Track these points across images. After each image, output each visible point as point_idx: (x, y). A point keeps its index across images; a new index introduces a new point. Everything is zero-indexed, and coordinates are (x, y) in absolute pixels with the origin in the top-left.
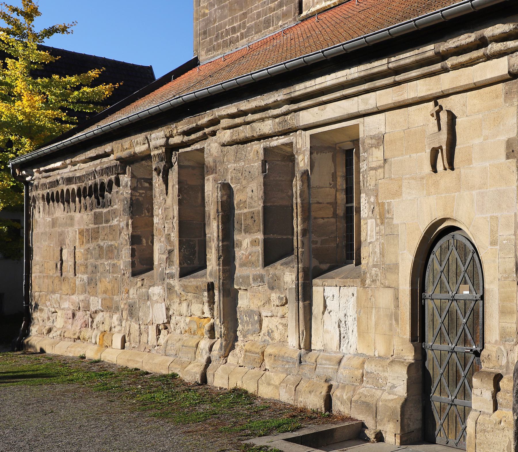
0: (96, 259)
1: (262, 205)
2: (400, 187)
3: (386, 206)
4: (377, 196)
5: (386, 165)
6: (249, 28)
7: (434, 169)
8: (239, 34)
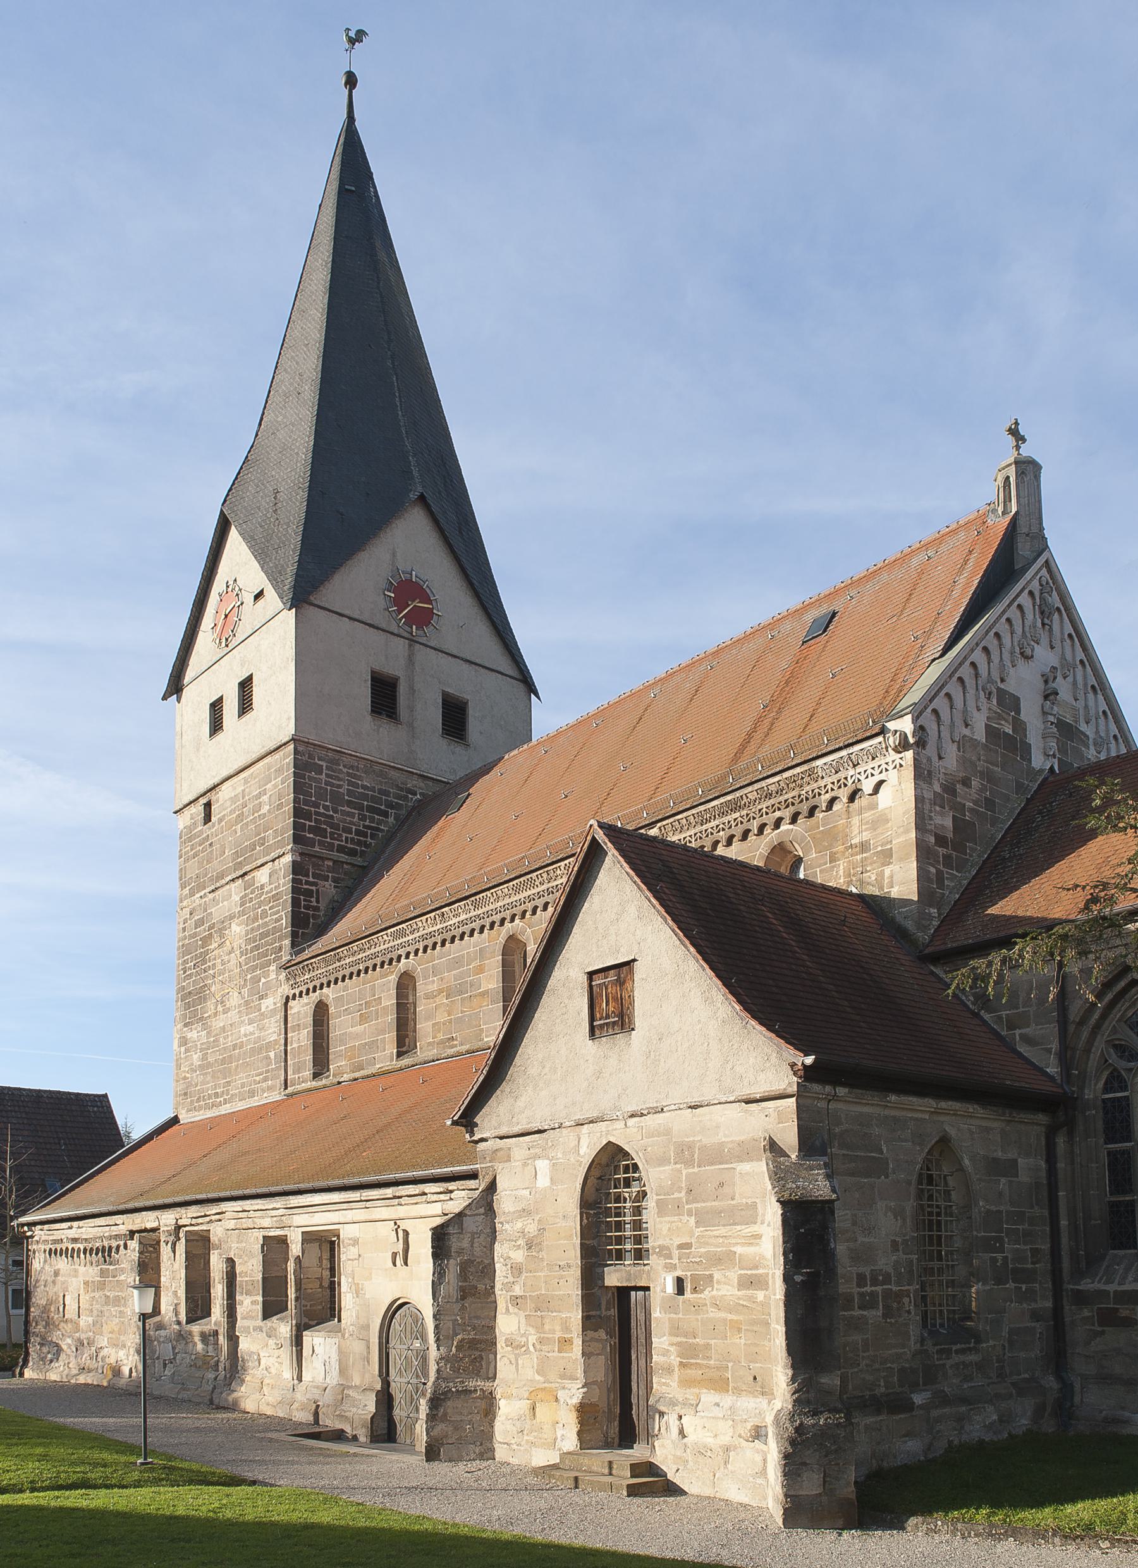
1: (261, 1276)
2: (371, 1274)
3: (360, 1286)
4: (353, 1278)
6: (232, 1095)
7: (394, 1264)
8: (222, 1099)
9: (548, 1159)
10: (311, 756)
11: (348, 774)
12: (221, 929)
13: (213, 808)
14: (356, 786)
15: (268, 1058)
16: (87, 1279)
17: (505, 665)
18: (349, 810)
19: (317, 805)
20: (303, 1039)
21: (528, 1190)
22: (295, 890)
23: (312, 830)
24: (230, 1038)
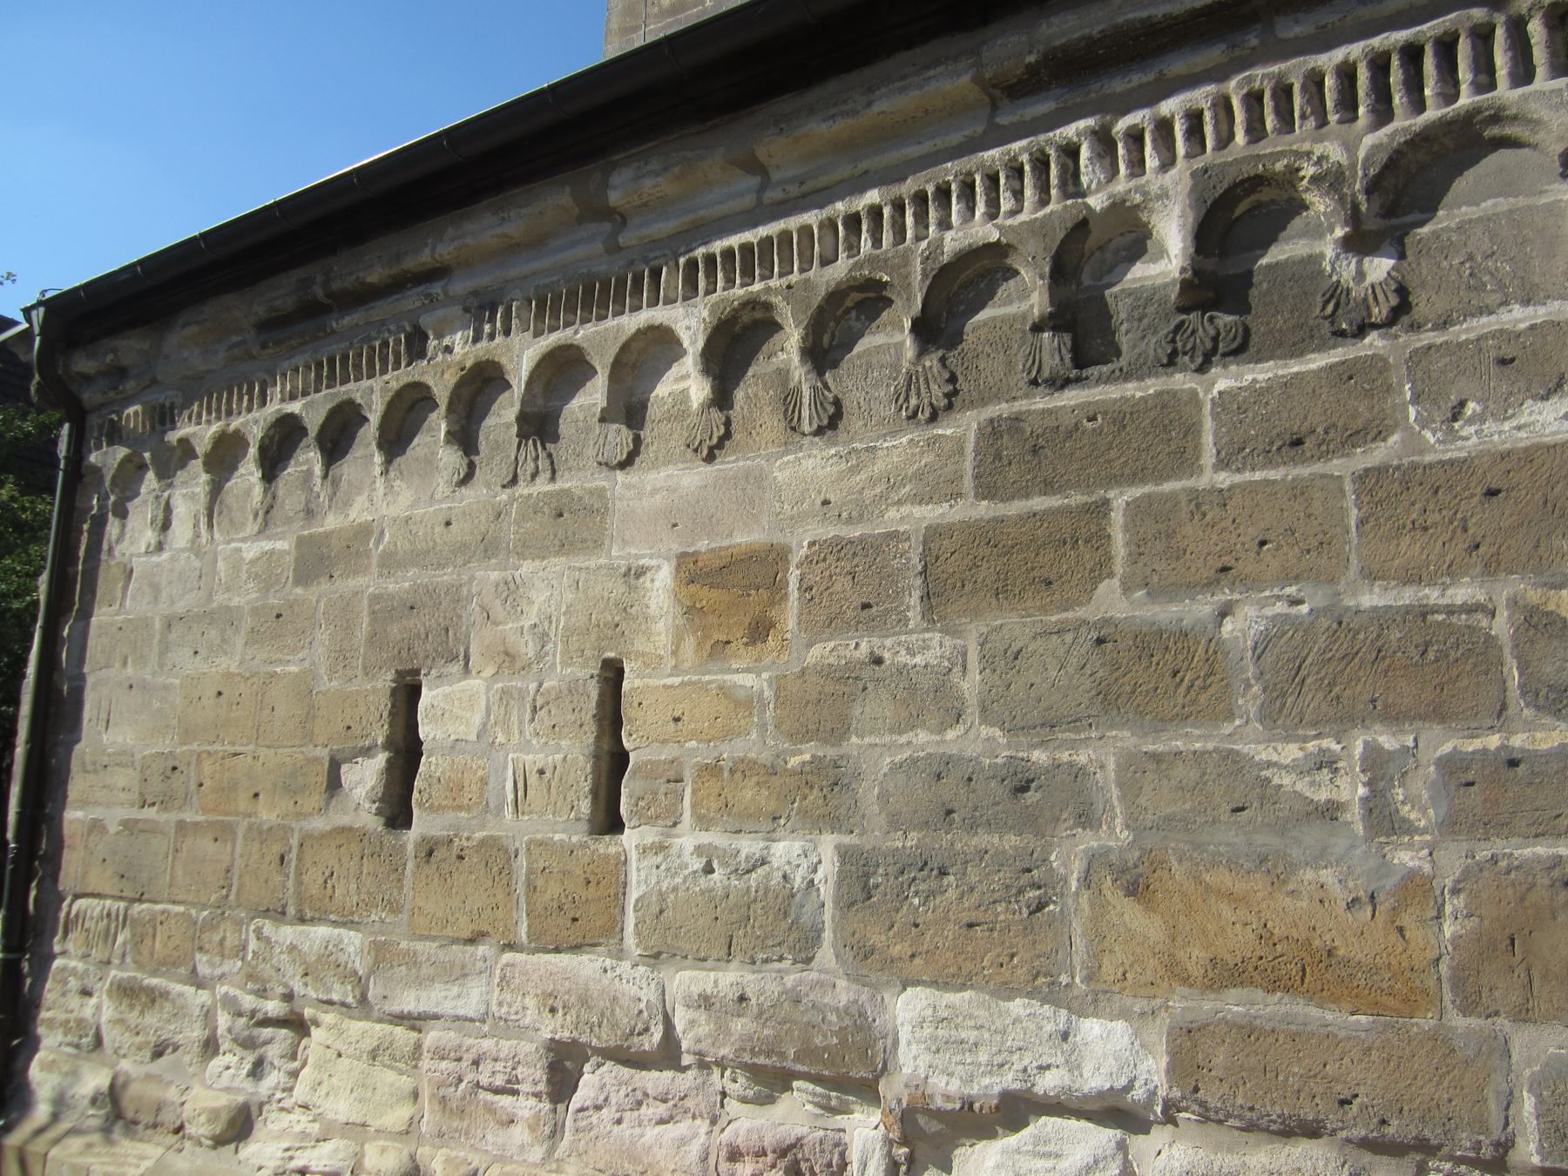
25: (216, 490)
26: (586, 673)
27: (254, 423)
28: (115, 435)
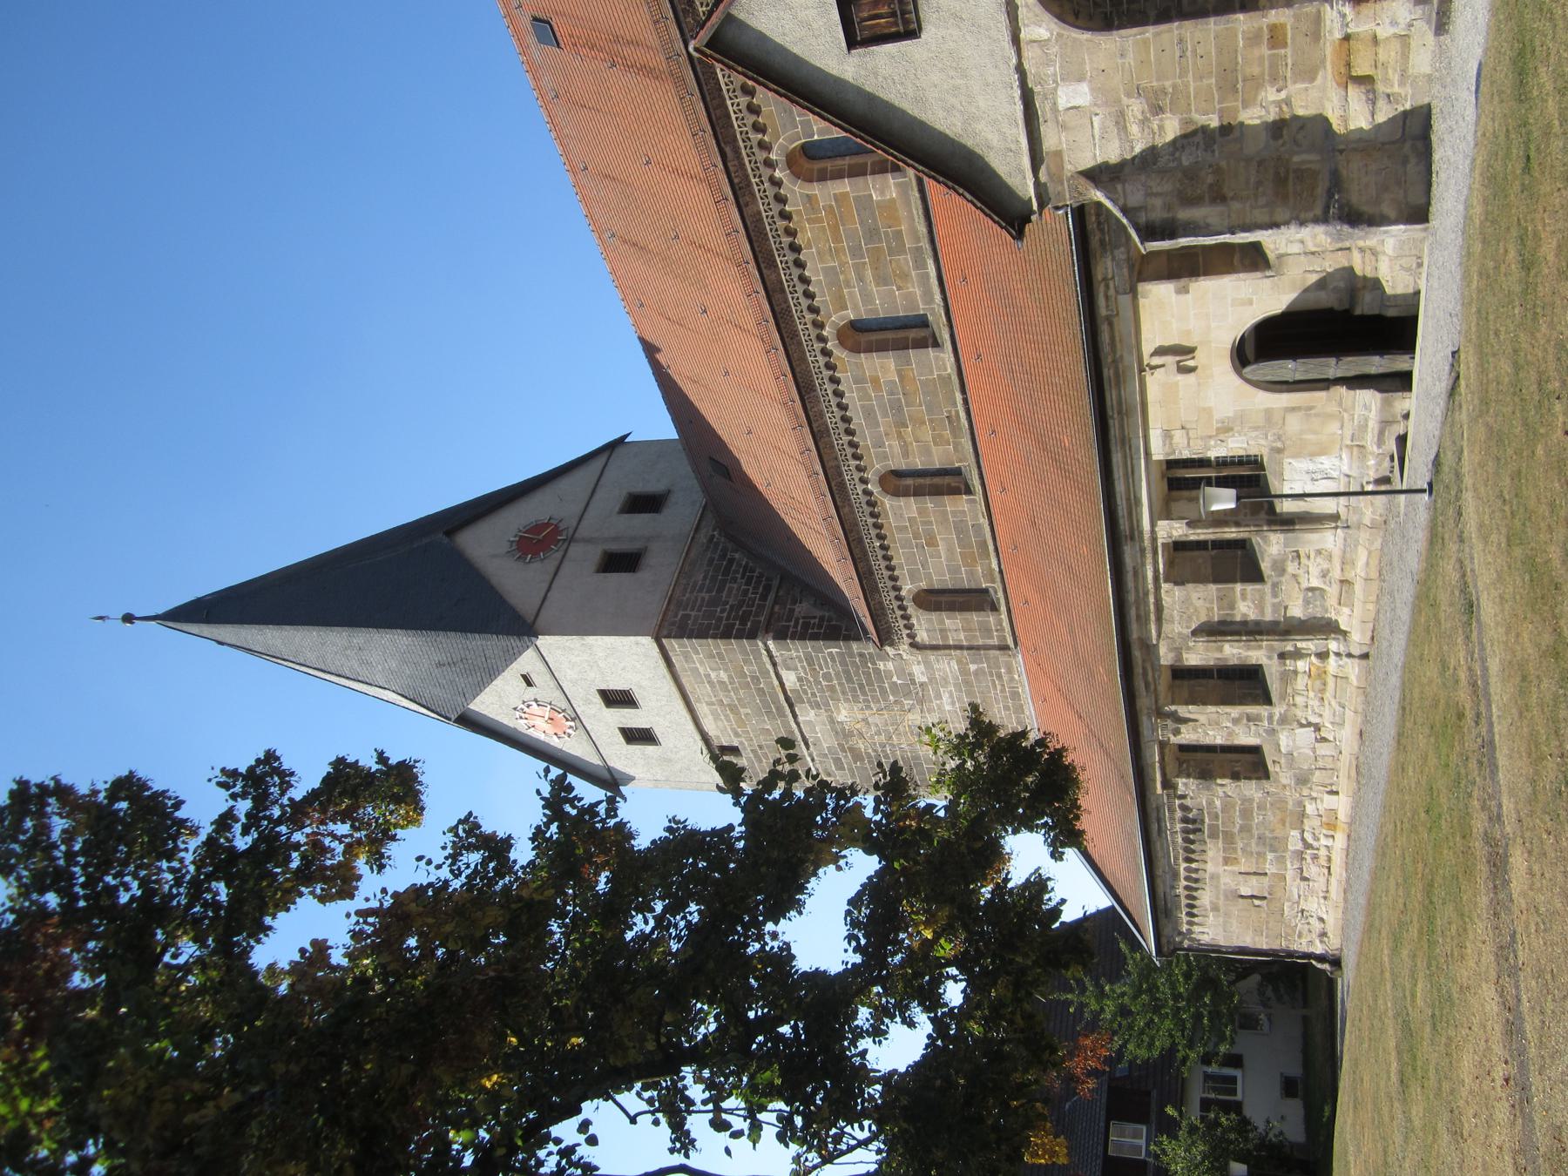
0: (1252, 836)
5: (1188, 427)
9: (1055, 89)
10: (673, 624)
11: (692, 592)
12: (843, 734)
13: (725, 744)
14: (703, 585)
15: (976, 673)
16: (1221, 859)
17: (597, 464)
18: (725, 592)
19: (720, 619)
20: (954, 625)
21: (1094, 118)
22: (802, 637)
23: (743, 623)
24: (957, 725)
25: (1197, 924)
26: (1240, 876)
27: (1185, 918)
28: (1181, 942)
